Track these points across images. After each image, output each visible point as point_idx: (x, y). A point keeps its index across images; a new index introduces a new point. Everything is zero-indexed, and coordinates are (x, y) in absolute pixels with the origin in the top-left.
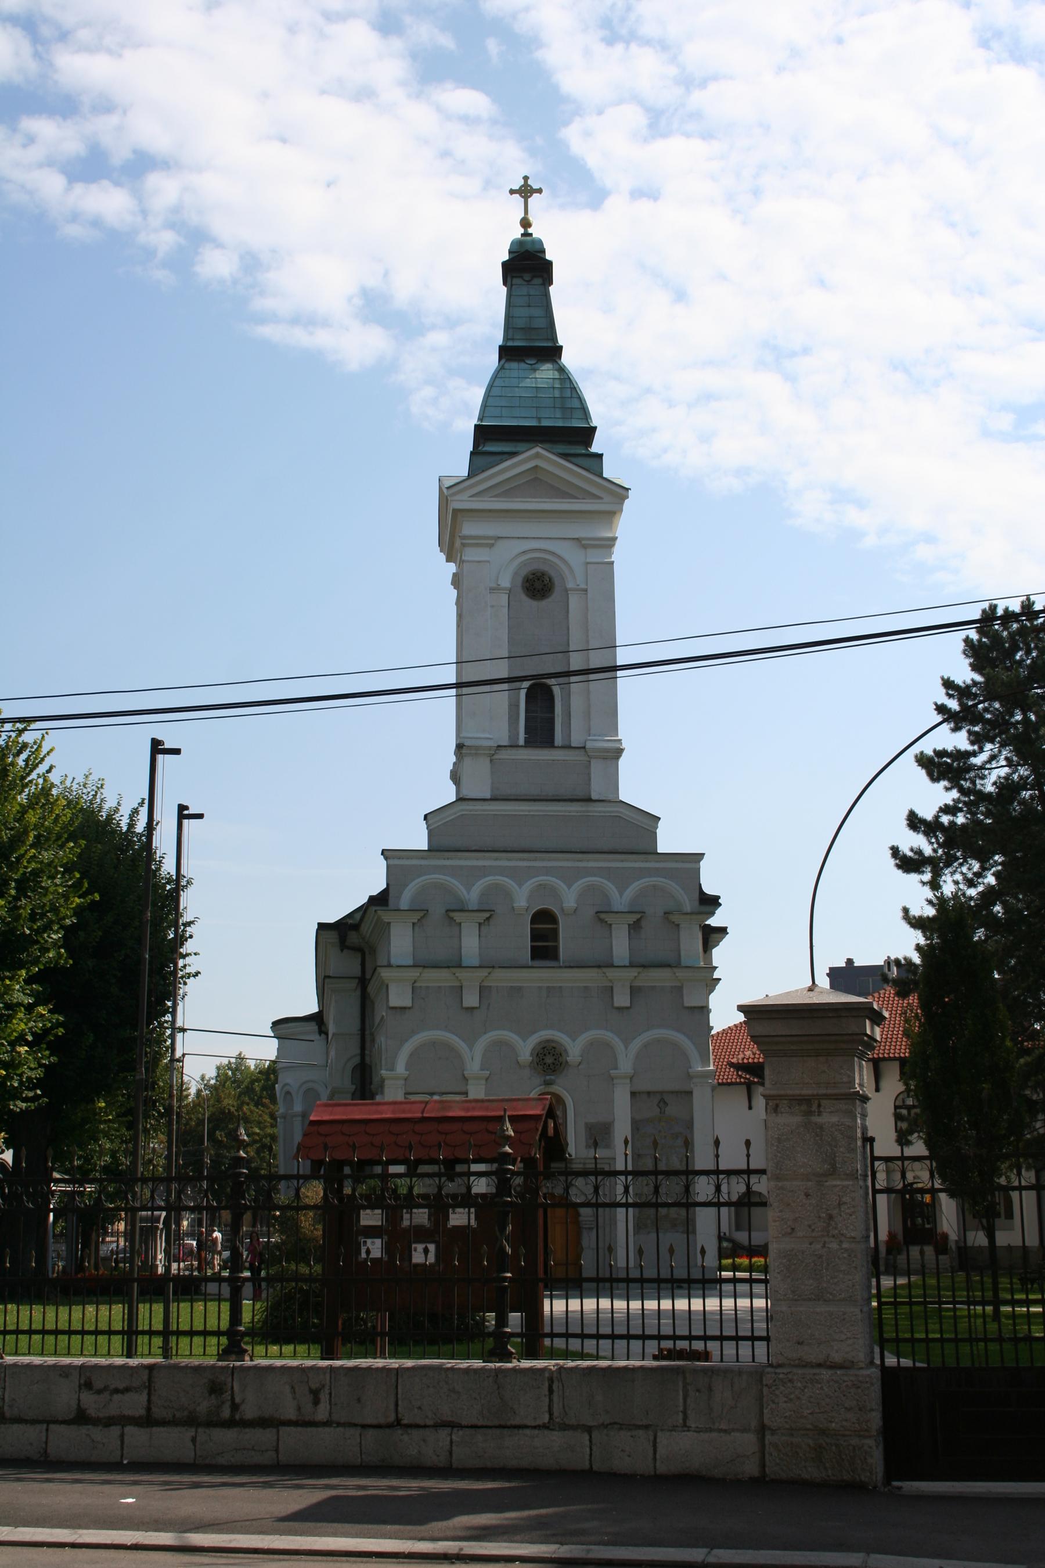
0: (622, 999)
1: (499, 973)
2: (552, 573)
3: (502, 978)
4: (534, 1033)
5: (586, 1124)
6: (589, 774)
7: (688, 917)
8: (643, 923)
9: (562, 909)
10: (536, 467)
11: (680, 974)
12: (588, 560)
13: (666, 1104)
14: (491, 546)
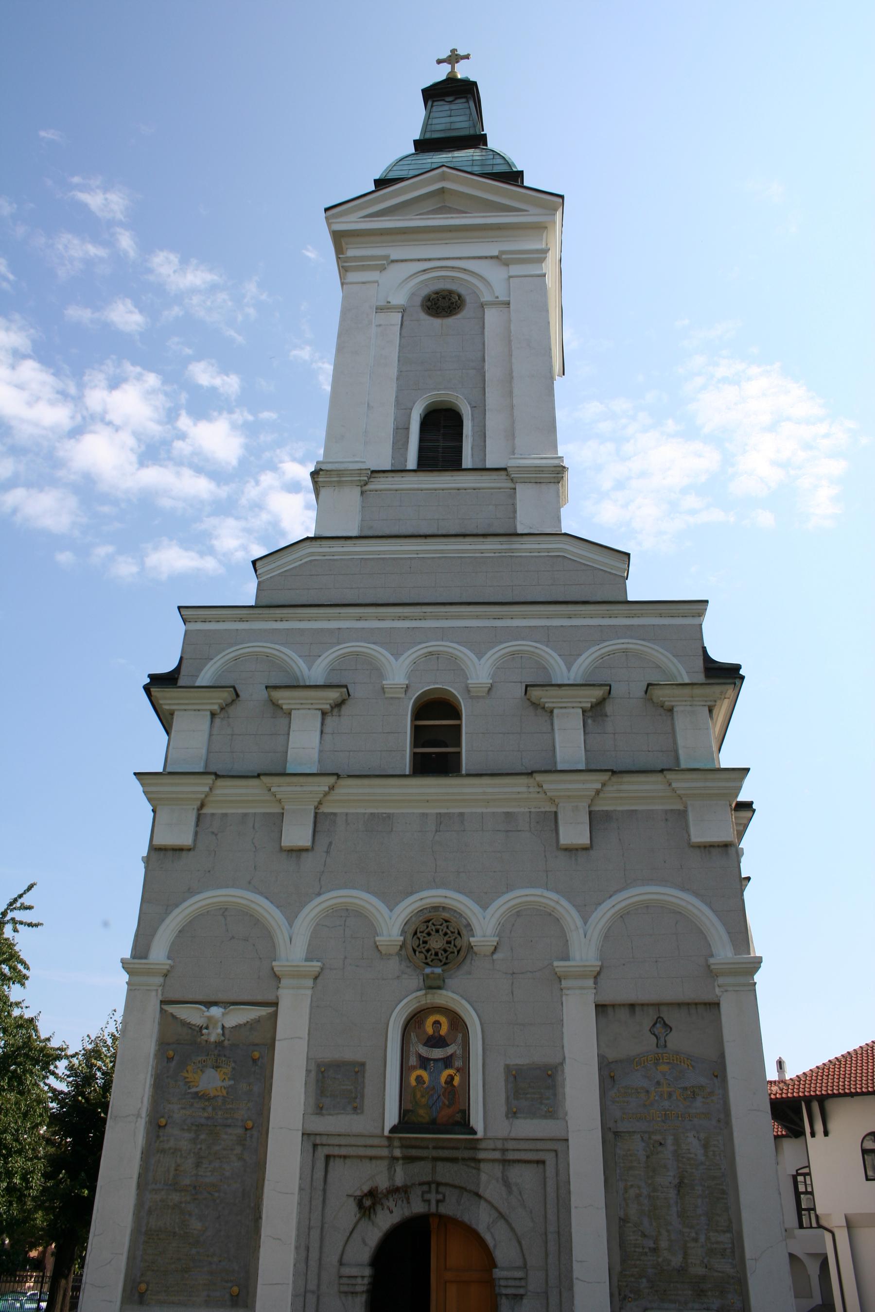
0: (573, 832)
1: (348, 789)
2: (462, 291)
3: (353, 799)
4: (412, 893)
5: (508, 1068)
6: (514, 505)
7: (687, 690)
8: (609, 708)
9: (468, 690)
10: (442, 191)
11: (681, 783)
12: (511, 274)
13: (668, 1027)
14: (382, 269)
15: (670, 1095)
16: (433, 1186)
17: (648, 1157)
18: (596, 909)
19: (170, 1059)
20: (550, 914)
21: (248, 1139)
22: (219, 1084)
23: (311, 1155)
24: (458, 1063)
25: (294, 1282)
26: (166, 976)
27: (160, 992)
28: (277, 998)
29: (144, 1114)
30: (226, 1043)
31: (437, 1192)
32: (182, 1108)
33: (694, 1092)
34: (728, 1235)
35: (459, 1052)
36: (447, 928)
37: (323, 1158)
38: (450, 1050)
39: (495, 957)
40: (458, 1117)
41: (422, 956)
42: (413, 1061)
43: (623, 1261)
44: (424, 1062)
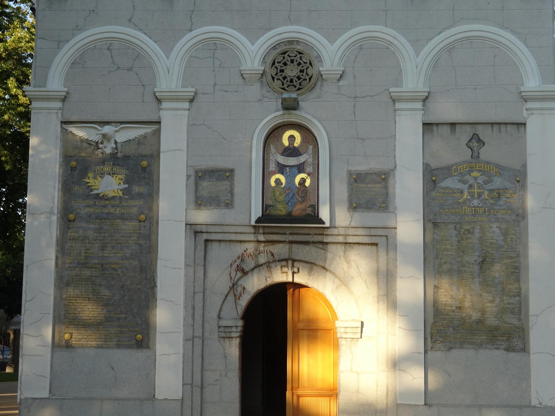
4: (270, 29)
5: (350, 173)
15: (480, 195)
16: (290, 263)
17: (458, 242)
18: (427, 44)
19: (73, 169)
20: (388, 48)
21: (142, 228)
22: (116, 187)
23: (194, 240)
24: (309, 169)
25: (184, 331)
26: (64, 100)
27: (60, 115)
28: (160, 117)
29: (56, 212)
30: (119, 155)
31: (293, 266)
32: (87, 206)
33: (499, 193)
34: (517, 298)
35: (310, 160)
36: (301, 59)
37: (203, 242)
38: (302, 159)
39: (341, 83)
40: (309, 211)
41: (279, 82)
42: (272, 167)
43: (435, 316)
44: (281, 169)
